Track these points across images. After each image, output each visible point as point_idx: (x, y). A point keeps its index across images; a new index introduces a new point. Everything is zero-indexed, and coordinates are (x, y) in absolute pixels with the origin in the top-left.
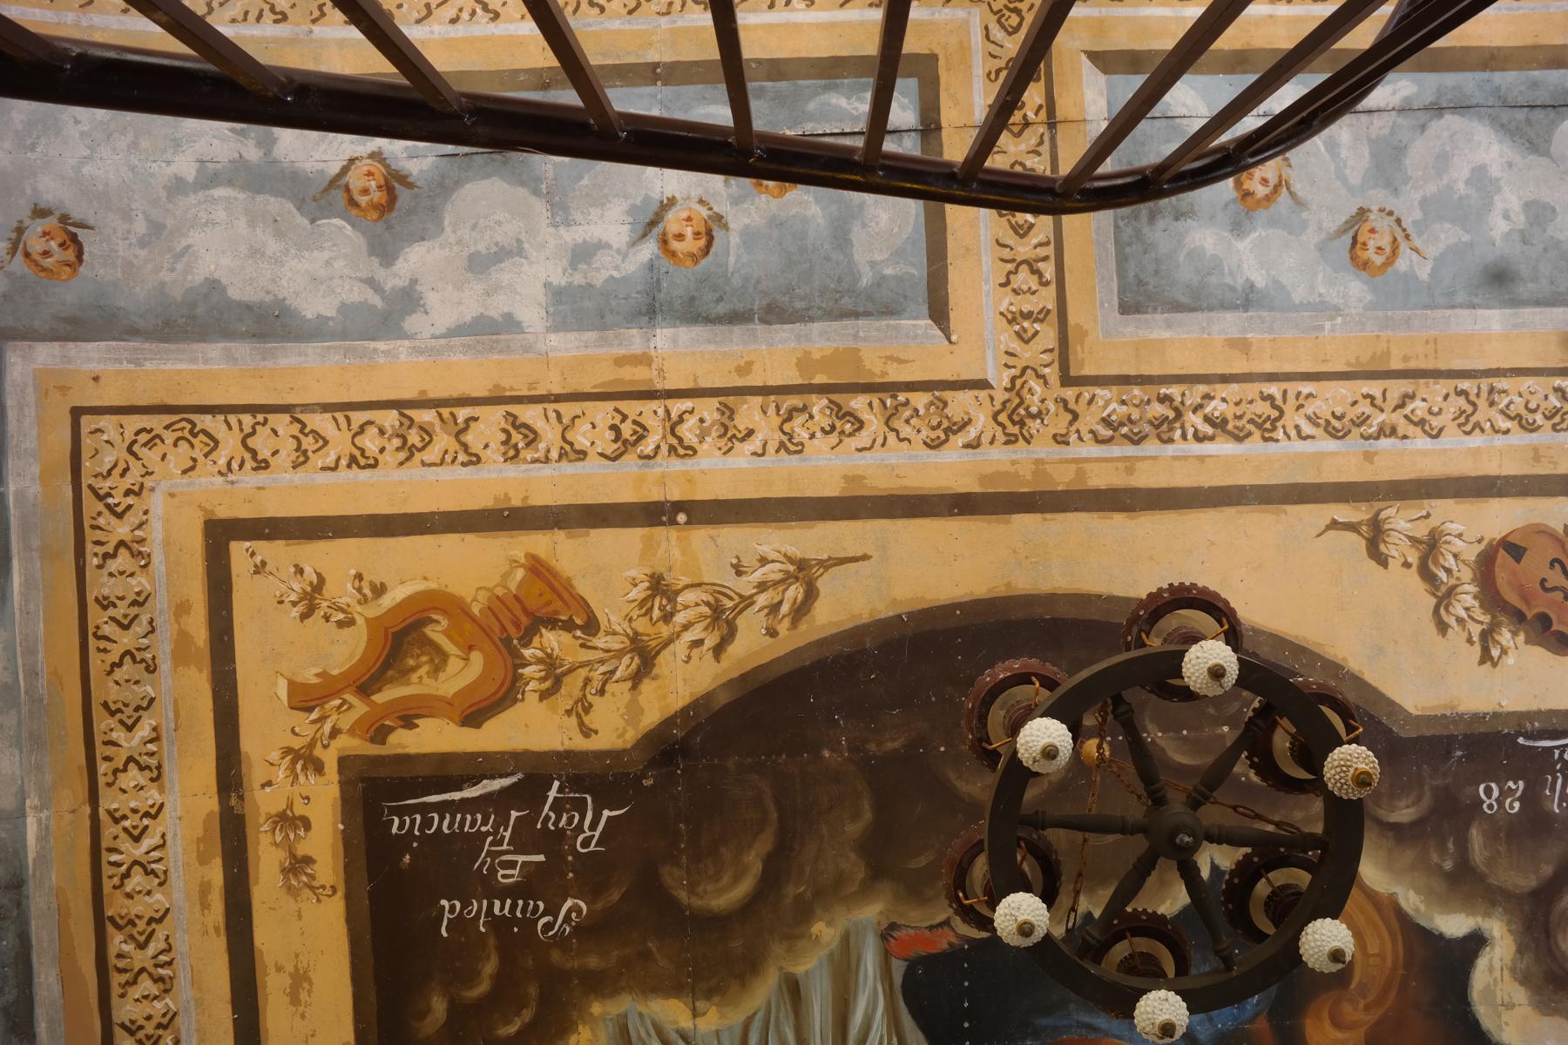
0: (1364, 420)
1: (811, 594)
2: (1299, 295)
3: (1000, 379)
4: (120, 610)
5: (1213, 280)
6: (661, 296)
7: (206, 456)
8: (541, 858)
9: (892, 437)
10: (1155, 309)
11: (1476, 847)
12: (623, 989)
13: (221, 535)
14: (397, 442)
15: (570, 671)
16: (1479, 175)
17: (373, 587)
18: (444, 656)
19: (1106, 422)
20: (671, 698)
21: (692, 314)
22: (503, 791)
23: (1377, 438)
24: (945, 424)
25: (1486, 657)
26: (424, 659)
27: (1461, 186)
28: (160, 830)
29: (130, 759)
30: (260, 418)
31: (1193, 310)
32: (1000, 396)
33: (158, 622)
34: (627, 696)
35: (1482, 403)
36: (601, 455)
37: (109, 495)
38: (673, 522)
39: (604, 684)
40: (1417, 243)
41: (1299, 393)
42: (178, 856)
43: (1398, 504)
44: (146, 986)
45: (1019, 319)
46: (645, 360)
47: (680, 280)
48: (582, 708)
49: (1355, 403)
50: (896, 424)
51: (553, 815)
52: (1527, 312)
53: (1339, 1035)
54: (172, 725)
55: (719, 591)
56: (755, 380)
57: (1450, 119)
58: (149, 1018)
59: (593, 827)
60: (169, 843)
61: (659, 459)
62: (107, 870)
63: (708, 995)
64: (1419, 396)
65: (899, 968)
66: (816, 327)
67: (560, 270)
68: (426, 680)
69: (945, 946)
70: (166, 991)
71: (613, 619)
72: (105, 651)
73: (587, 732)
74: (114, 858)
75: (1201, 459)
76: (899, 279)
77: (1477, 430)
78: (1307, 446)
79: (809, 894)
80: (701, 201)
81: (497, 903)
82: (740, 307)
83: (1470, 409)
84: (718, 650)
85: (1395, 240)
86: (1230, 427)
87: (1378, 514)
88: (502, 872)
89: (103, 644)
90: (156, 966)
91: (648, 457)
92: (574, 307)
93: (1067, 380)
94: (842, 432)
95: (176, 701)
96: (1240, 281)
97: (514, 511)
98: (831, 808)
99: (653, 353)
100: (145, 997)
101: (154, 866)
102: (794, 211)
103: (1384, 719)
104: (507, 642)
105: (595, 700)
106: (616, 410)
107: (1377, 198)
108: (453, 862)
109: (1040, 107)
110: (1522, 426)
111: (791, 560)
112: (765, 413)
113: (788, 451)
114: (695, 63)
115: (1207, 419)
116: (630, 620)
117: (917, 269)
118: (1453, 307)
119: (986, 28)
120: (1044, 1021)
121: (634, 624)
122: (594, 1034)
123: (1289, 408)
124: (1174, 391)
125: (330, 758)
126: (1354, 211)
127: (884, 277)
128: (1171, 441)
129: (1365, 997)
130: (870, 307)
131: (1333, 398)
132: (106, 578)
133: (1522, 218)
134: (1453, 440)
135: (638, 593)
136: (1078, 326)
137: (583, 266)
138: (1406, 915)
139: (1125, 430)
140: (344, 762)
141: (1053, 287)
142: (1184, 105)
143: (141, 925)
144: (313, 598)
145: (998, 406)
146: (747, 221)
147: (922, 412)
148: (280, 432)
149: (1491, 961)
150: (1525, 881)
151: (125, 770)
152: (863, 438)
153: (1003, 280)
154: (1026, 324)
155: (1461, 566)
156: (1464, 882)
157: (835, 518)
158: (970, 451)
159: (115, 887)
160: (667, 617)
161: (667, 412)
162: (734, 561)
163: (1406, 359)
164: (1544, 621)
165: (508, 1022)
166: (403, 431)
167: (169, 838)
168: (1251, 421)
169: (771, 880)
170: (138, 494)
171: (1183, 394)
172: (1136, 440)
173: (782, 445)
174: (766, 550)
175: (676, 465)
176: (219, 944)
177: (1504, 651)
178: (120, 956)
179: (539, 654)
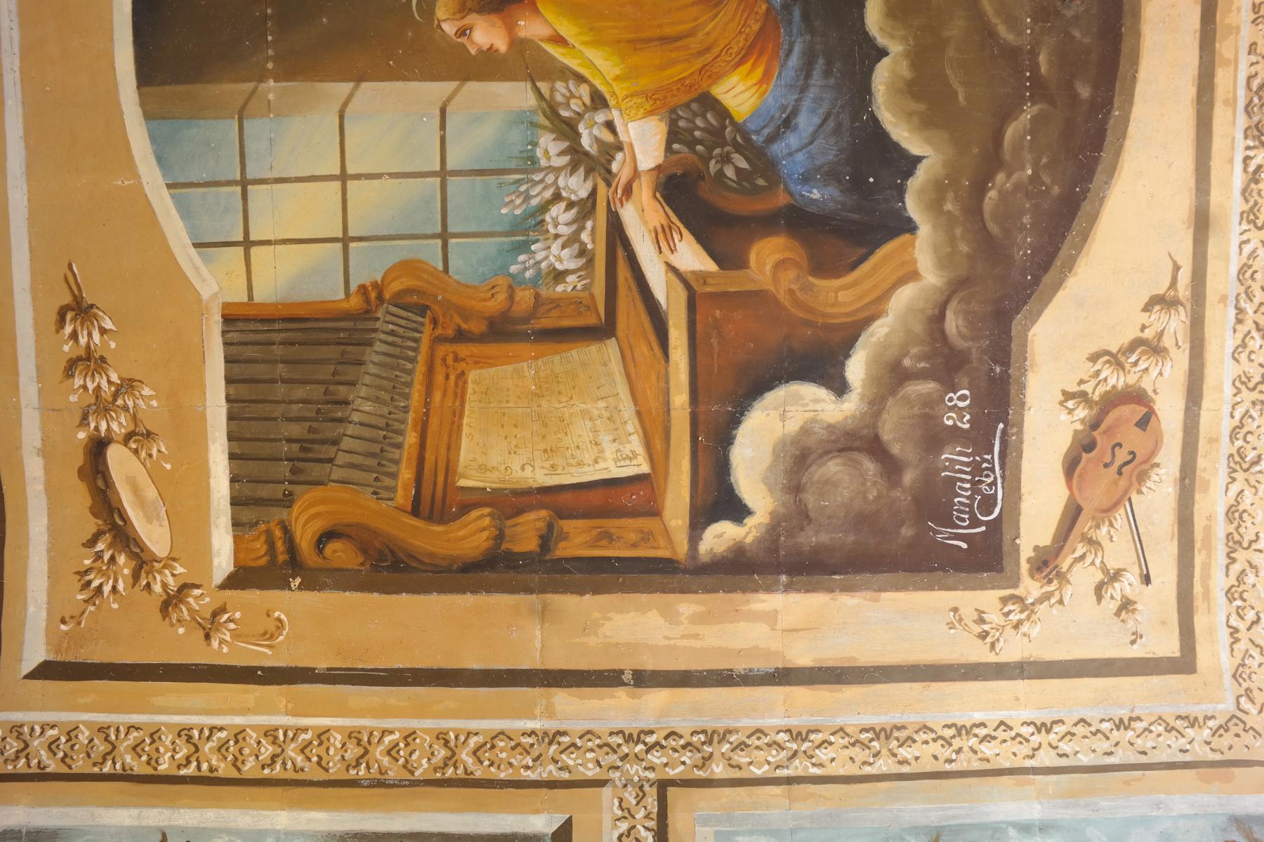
11: (919, 387)
23: (1236, 308)
25: (1068, 396)
35: (1255, 395)
53: (768, 268)
75: (1231, 161)
78: (1234, 249)
83: (1251, 385)
86: (1253, 186)
87: (1182, 305)
103: (1027, 307)
120: (797, 13)
128: (1246, 137)
129: (801, 289)
149: (824, 401)
150: (890, 430)
155: (1138, 375)
156: (893, 376)
164: (1090, 447)
168: (1256, 203)
177: (1071, 411)
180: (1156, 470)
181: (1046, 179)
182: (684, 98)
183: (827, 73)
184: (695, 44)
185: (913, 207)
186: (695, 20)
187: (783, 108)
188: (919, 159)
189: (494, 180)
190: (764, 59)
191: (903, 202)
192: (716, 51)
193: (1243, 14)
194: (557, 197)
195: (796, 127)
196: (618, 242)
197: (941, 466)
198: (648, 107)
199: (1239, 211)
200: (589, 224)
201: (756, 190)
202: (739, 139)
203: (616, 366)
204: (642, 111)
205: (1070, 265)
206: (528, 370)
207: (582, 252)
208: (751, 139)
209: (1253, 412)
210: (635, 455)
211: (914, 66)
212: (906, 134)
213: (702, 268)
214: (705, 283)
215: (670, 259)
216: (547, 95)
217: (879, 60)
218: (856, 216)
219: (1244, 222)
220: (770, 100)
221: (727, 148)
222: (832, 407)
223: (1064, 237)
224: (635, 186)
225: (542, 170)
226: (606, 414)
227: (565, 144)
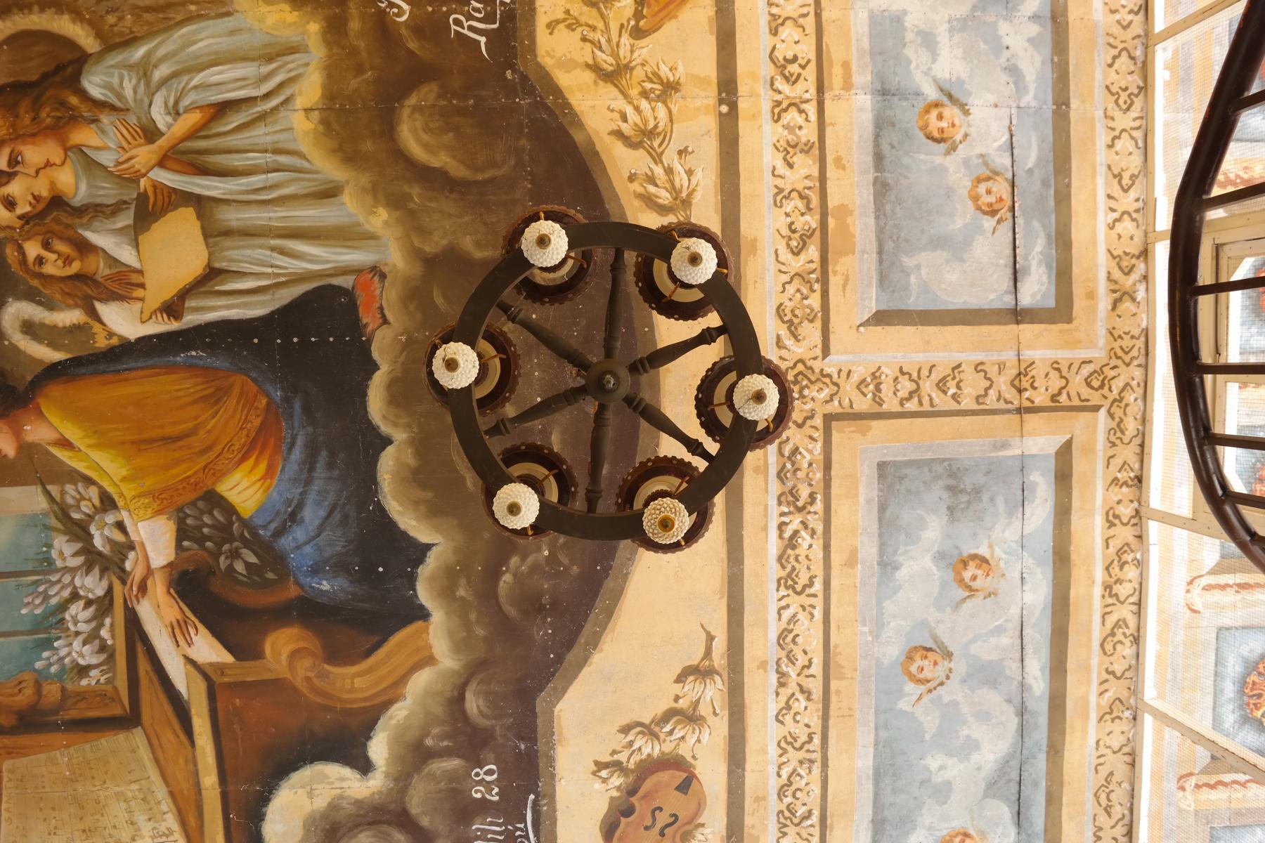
0: (792, 660)
2: (889, 606)
5: (902, 537)
6: (896, 98)
9: (786, 278)
10: (881, 490)
12: (331, 50)
15: (602, 15)
16: (973, 746)
19: (796, 450)
20: (579, 96)
21: (882, 124)
23: (778, 672)
24: (796, 321)
25: (600, 766)
27: (966, 732)
31: (880, 520)
32: (817, 365)
34: (581, 60)
35: (802, 755)
36: (774, 48)
39: (590, 41)
40: (925, 699)
41: (814, 607)
43: (726, 690)
45: (875, 382)
46: (848, 85)
47: (907, 114)
48: (572, 23)
49: (805, 652)
50: (797, 281)
52: (869, 787)
53: (284, 657)
55: (666, 136)
56: (831, 172)
57: (1014, 722)
59: (471, 28)
61: (771, 92)
63: (325, 122)
64: (810, 704)
65: (346, 282)
66: (872, 221)
67: (916, 22)
69: (364, 321)
71: (644, 51)
73: (552, 26)
75: (765, 528)
76: (906, 288)
77: (781, 752)
79: (412, 205)
80: (966, 135)
82: (887, 162)
83: (797, 745)
84: (618, 134)
85: (928, 681)
86: (790, 551)
91: (772, 84)
92: (888, 30)
93: (829, 419)
94: (790, 239)
96: (900, 559)
98: (485, 224)
99: (852, 92)
102: (958, 206)
103: (551, 685)
105: (577, 35)
106: (809, 61)
107: (960, 666)
109: (1033, 402)
110: (783, 787)
111: (690, 194)
112: (806, 178)
113: (777, 194)
114: (1068, 136)
115: (796, 533)
116: (643, 65)
117: (914, 302)
118: (876, 729)
119: (1090, 362)
120: (297, 406)
121: (639, 67)
122: (290, 25)
123: (803, 599)
124: (819, 506)
126: (951, 649)
127: (908, 275)
128: (780, 503)
129: (317, 677)
130: (886, 264)
131: (810, 635)
133: (940, 780)
134: (775, 732)
135: (664, 71)
136: (870, 428)
137: (919, 40)
138: (387, 709)
139: (789, 466)
141: (899, 409)
142: (1032, 514)
145: (809, 363)
146: (951, 170)
147: (805, 302)
150: (415, 808)
152: (785, 255)
153: (905, 370)
154: (871, 387)
156: (415, 755)
158: (775, 340)
160: (645, 94)
161: (807, 101)
162: (690, 149)
163: (838, 692)
164: (628, 811)
168: (794, 569)
171: (816, 513)
172: (781, 476)
173: (781, 190)
174: (698, 175)
175: (766, 106)
177: (605, 780)
180: (701, 830)
181: (566, 561)
182: (190, 497)
183: (331, 465)
184: (196, 442)
185: (424, 594)
186: (196, 418)
187: (288, 502)
188: (428, 547)
189: (12, 582)
190: (267, 454)
191: (415, 590)
192: (218, 448)
194: (75, 596)
195: (302, 521)
196: (137, 637)
197: (472, 835)
198: (155, 506)
199: (775, 577)
200: (108, 621)
201: (267, 584)
202: (246, 534)
203: (144, 752)
204: (150, 510)
205: (594, 642)
206: (62, 757)
207: (103, 648)
208: (258, 534)
209: (799, 770)
210: (171, 832)
211: (418, 453)
212: (414, 523)
213: (219, 660)
214: (223, 674)
215: (188, 652)
216: (58, 498)
217: (383, 449)
218: (367, 606)
219: (782, 588)
220: (275, 494)
221: (236, 544)
222: (357, 784)
223: (587, 615)
224: (149, 583)
225: (57, 570)
226: (141, 796)
227: (78, 546)
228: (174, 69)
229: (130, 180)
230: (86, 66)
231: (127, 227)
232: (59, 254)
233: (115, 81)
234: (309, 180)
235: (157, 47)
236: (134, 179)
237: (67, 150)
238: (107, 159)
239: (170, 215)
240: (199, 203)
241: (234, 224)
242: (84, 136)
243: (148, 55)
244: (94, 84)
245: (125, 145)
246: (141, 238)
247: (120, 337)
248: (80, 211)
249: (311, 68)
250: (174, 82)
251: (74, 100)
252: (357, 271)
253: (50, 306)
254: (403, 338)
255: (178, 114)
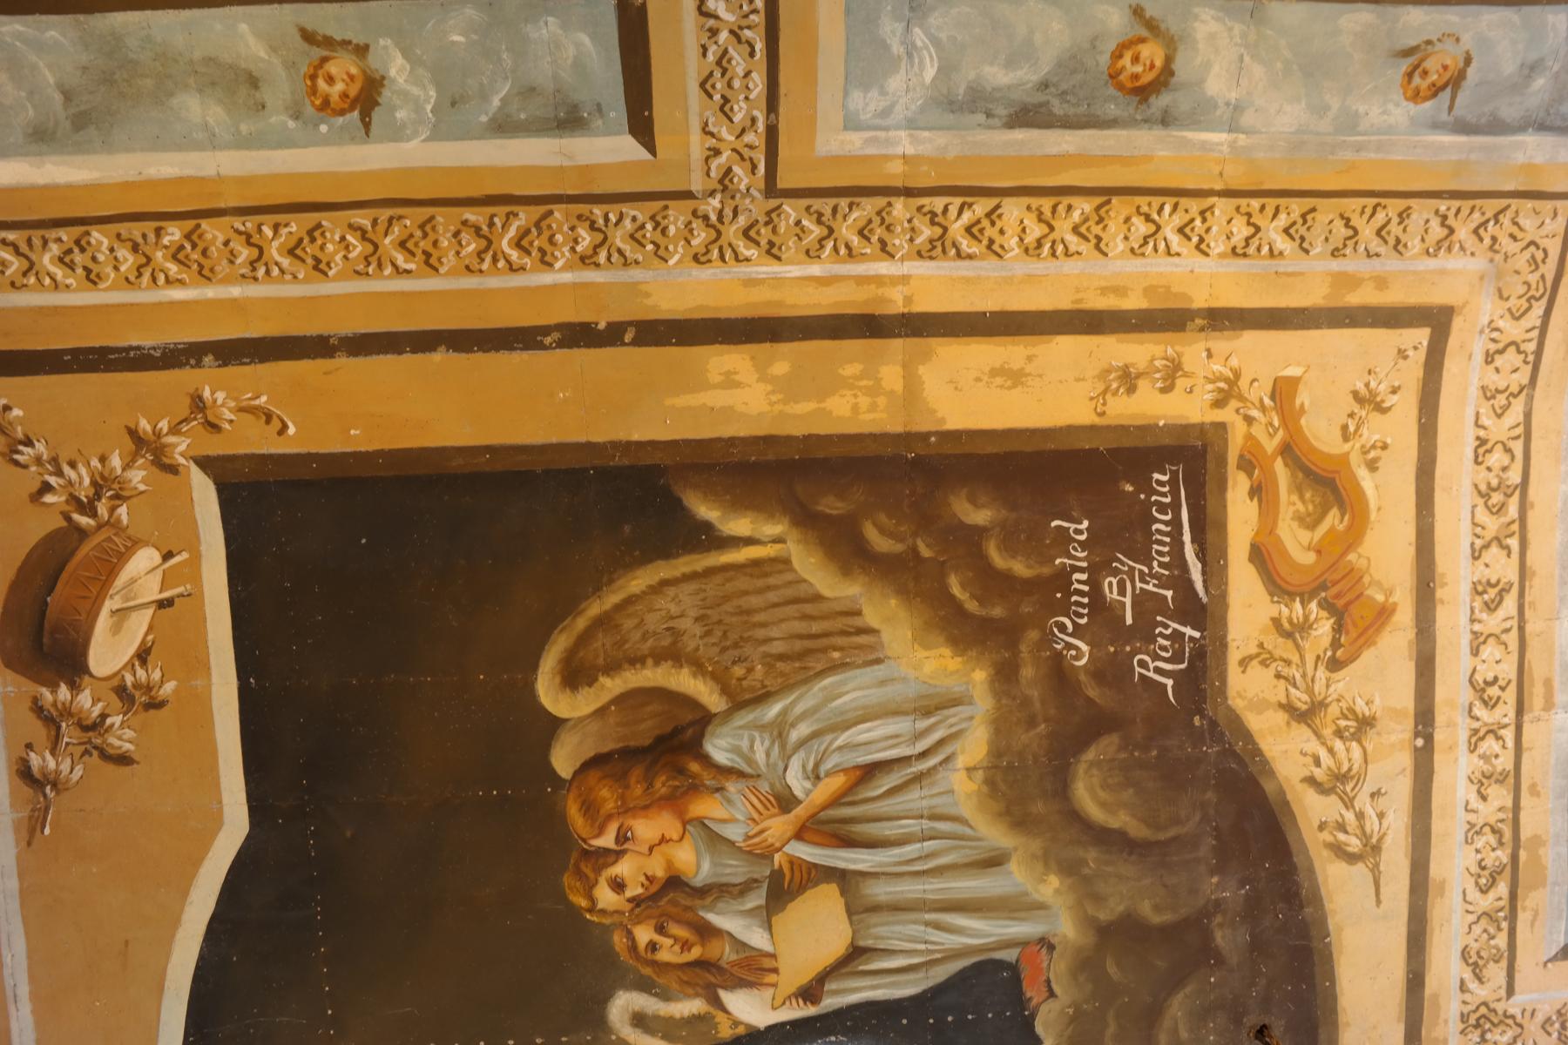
1: (1352, 858)
3: (1514, 1007)
4: (1395, 229)
7: (1509, 310)
8: (1129, 621)
12: (999, 701)
13: (1438, 321)
14: (1495, 482)
15: (1298, 647)
17: (1375, 460)
18: (1312, 527)
22: (1190, 583)
26: (1311, 507)
28: (1184, 251)
29: (1258, 229)
30: (1531, 358)
33: (1375, 261)
34: (1274, 699)
36: (1474, 670)
37: (1497, 222)
38: (1417, 735)
39: (1286, 679)
42: (1156, 266)
44: (1035, 230)
48: (1265, 657)
50: (1484, 922)
51: (1168, 632)
54: (1281, 270)
55: (1360, 778)
58: (1002, 232)
59: (1158, 670)
60: (1170, 259)
61: (1468, 720)
62: (1157, 201)
63: (990, 782)
65: (1010, 955)
68: (1292, 508)
69: (1028, 995)
70: (1027, 250)
71: (1341, 685)
72: (1363, 212)
73: (1244, 663)
74: (1167, 209)
79: (1086, 871)
81: (1084, 577)
84: (1311, 781)
88: (1115, 581)
89: (1368, 211)
90: (1054, 242)
91: (1470, 710)
95: (1301, 274)
97: (1432, 592)
98: (1165, 886)
100: (1024, 230)
101: (1151, 244)
104: (1323, 587)
105: (1271, 671)
108: (1124, 534)
111: (1380, 839)
122: (952, 673)
125: (1226, 415)
132: (1425, 216)
135: (1361, 707)
140: (1221, 427)
143: (1097, 230)
144: (1370, 402)
145: (1492, 1006)
148: (1515, 376)
151: (1249, 223)
152: (1473, 894)
157: (1412, 874)
159: (1138, 207)
160: (1339, 733)
161: (1505, 726)
165: (963, 586)
166: (1503, 488)
167: (1176, 260)
169: (1104, 837)
170: (1491, 248)
173: (1472, 826)
174: (1390, 817)
175: (1463, 736)
176: (1065, 303)
178: (1070, 207)
179: (1313, 617)
193: (1451, 1024)
228: (815, 727)
229: (762, 856)
230: (710, 728)
231: (758, 908)
232: (676, 939)
233: (745, 744)
234: (971, 848)
235: (793, 703)
236: (766, 855)
237: (685, 824)
238: (734, 833)
239: (809, 893)
240: (843, 879)
241: (883, 898)
242: (706, 807)
243: (784, 712)
244: (719, 748)
245: (756, 816)
246: (774, 919)
247: (748, 1026)
248: (702, 892)
249: (975, 722)
250: (815, 744)
251: (694, 767)
252: (1023, 944)
253: (666, 996)
254: (1071, 1011)
255: (818, 778)
